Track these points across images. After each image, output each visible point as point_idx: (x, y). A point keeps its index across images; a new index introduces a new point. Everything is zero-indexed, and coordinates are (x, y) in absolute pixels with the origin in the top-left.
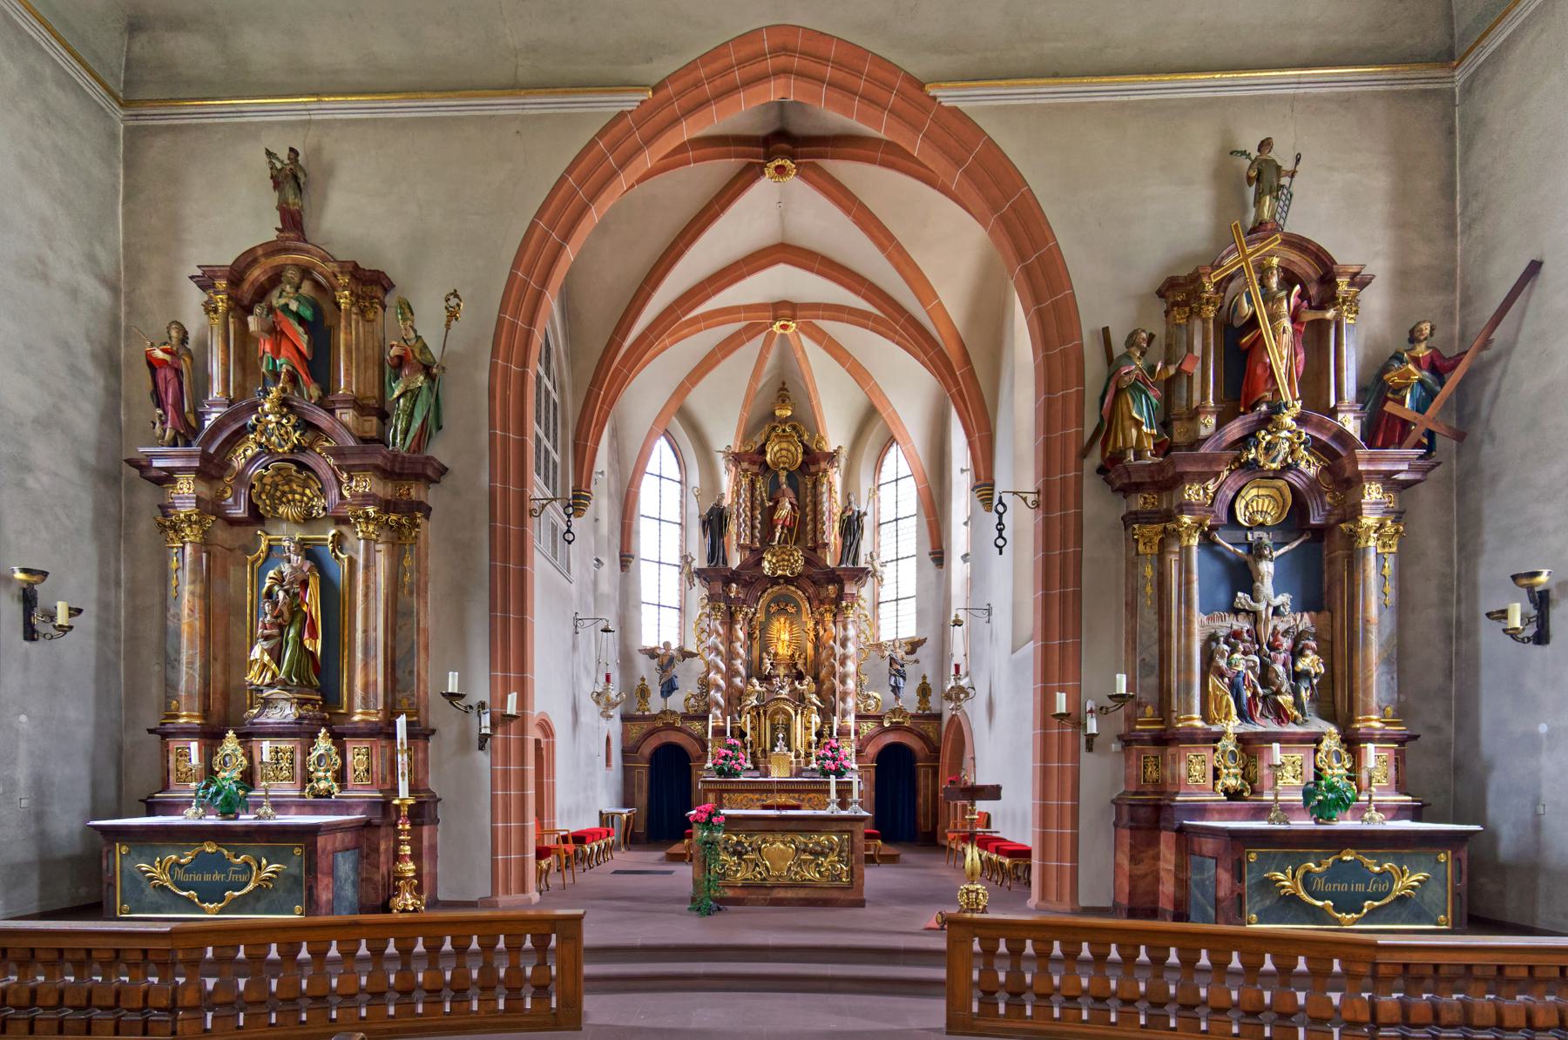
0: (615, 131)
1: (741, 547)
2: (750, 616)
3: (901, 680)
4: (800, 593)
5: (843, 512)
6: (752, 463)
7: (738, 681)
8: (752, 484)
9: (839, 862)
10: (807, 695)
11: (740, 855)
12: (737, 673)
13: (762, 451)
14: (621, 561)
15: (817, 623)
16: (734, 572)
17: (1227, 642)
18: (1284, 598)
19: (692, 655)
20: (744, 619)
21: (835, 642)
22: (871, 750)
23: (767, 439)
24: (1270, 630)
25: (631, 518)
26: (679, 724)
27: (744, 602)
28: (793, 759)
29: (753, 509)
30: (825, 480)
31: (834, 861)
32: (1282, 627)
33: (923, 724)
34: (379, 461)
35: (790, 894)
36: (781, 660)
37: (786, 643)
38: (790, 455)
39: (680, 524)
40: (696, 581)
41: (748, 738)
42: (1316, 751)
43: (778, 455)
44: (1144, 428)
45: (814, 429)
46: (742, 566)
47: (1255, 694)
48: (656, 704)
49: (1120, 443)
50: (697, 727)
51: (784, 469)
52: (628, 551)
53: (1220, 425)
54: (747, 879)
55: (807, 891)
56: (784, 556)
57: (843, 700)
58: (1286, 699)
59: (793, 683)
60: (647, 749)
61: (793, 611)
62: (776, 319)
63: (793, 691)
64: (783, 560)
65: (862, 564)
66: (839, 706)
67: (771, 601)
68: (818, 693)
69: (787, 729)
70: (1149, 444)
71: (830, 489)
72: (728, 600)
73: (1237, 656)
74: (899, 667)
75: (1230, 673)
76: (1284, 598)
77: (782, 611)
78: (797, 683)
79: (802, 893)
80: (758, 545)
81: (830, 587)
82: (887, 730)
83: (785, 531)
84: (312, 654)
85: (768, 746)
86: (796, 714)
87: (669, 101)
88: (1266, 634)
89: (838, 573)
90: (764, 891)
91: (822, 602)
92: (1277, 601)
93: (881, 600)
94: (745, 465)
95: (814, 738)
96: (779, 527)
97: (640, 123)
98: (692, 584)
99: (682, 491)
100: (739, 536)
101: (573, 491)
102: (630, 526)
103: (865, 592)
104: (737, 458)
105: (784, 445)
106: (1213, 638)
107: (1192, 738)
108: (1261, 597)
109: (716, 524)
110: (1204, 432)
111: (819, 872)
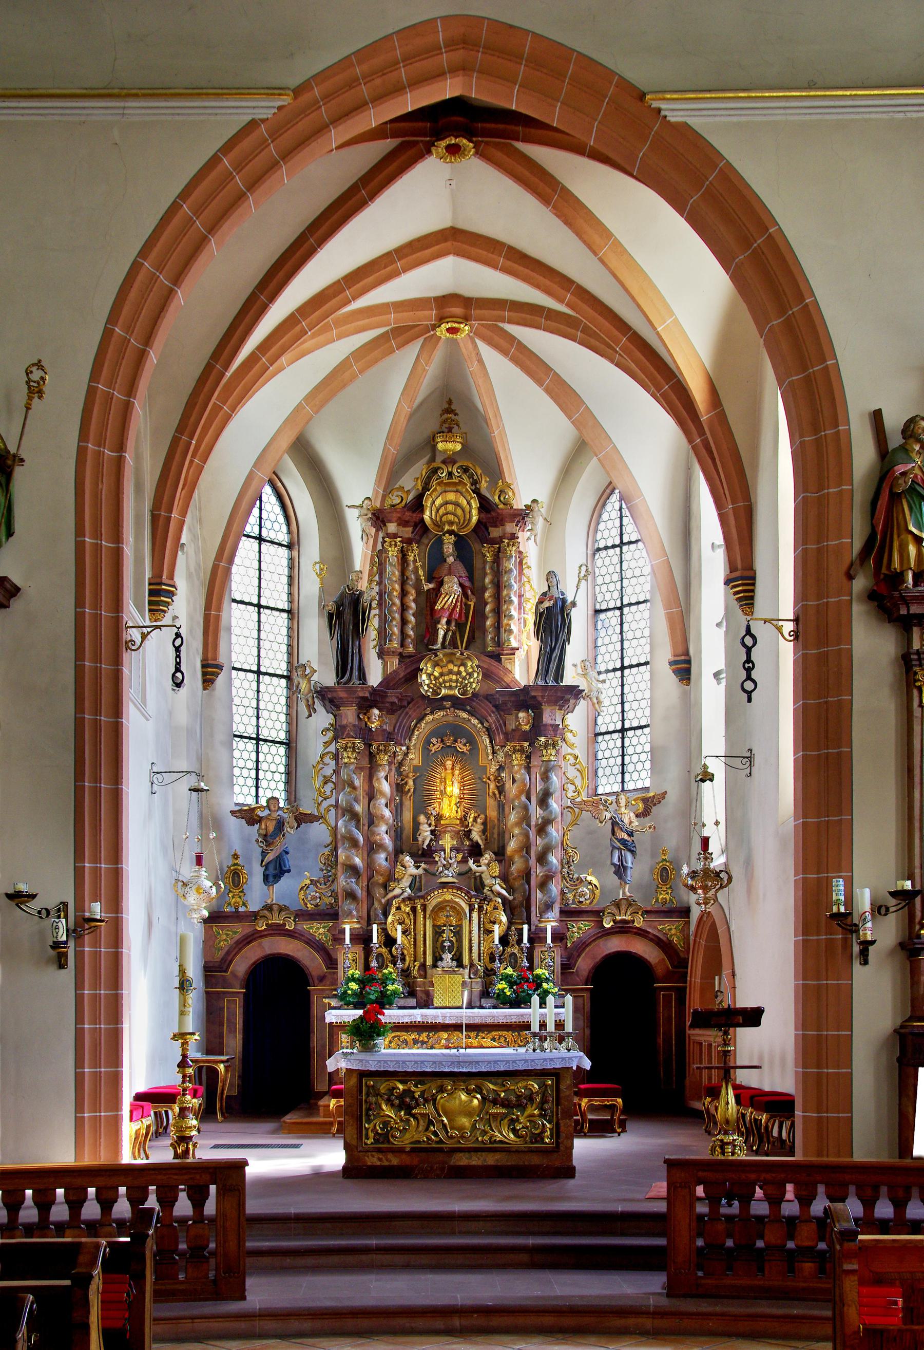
0: (246, 144)
1: (382, 654)
2: (400, 758)
3: (629, 856)
4: (475, 721)
5: (540, 602)
6: (403, 523)
9: (541, 1115)
10: (488, 881)
11: (408, 1109)
13: (417, 505)
15: (501, 768)
16: (374, 691)
20: (390, 763)
21: (529, 798)
23: (426, 488)
27: (389, 737)
28: (467, 978)
30: (513, 551)
31: (533, 1115)
33: (662, 923)
35: (476, 1160)
36: (447, 826)
37: (454, 800)
38: (459, 512)
39: (289, 612)
40: (318, 705)
43: (441, 511)
45: (496, 472)
46: (387, 682)
51: (451, 532)
54: (418, 1142)
55: (498, 1156)
56: (451, 666)
57: (543, 885)
59: (464, 861)
61: (465, 749)
62: (441, 319)
63: (466, 874)
64: (451, 672)
65: (570, 678)
66: (538, 896)
67: (433, 733)
68: (505, 878)
69: (458, 934)
71: (521, 563)
72: (366, 734)
74: (626, 837)
77: (448, 750)
78: (471, 862)
79: (491, 1159)
80: (411, 649)
81: (522, 715)
82: (608, 933)
83: (453, 627)
85: (429, 961)
86: (471, 910)
87: (314, 105)
89: (533, 694)
90: (440, 1157)
91: (508, 737)
93: (597, 731)
94: (392, 527)
96: (444, 621)
97: (275, 134)
98: (311, 709)
99: (291, 559)
100: (383, 634)
101: (150, 584)
102: (218, 618)
104: (378, 518)
105: (451, 496)
111: (515, 1131)
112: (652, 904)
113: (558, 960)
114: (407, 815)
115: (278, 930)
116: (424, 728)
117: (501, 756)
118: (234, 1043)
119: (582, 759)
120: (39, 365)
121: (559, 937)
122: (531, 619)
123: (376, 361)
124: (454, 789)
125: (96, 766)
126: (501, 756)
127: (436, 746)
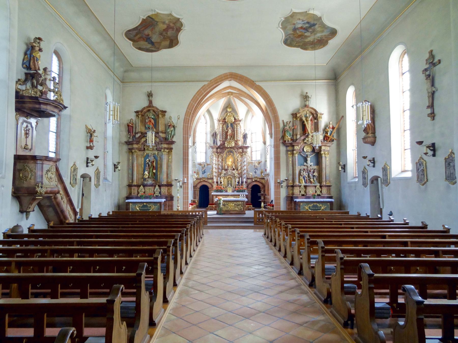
1: (220, 140)
7: (220, 171)
8: (223, 126)
10: (235, 174)
12: (220, 169)
14: (193, 144)
15: (237, 157)
16: (219, 146)
17: (303, 171)
18: (312, 164)
19: (209, 165)
22: (250, 186)
24: (310, 168)
25: (195, 134)
26: (206, 180)
27: (221, 153)
29: (223, 132)
32: (311, 168)
34: (167, 143)
37: (231, 162)
40: (210, 148)
41: (222, 183)
42: (316, 188)
44: (289, 137)
46: (221, 145)
47: (307, 179)
48: (201, 176)
49: (285, 140)
50: (210, 181)
51: (230, 123)
52: (195, 141)
53: (301, 136)
58: (312, 180)
59: (232, 171)
60: (199, 186)
61: (232, 154)
69: (231, 182)
70: (290, 140)
73: (304, 173)
75: (303, 176)
76: (312, 164)
77: (229, 154)
80: (224, 140)
81: (240, 150)
84: (154, 173)
85: (227, 186)
86: (233, 178)
88: (309, 169)
92: (310, 164)
95: (237, 184)
96: (229, 136)
102: (195, 136)
103: (249, 150)
106: (301, 170)
107: (296, 186)
108: (308, 163)
109: (215, 135)
110: (298, 138)
112: (260, 177)
113: (246, 186)
114: (224, 164)
115: (204, 181)
116: (226, 151)
117: (237, 155)
118: (198, 197)
119: (250, 156)
120: (179, 116)
121: (246, 182)
122: (242, 136)
123: (219, 100)
124: (230, 160)
125: (185, 163)
126: (237, 155)
127: (228, 154)
